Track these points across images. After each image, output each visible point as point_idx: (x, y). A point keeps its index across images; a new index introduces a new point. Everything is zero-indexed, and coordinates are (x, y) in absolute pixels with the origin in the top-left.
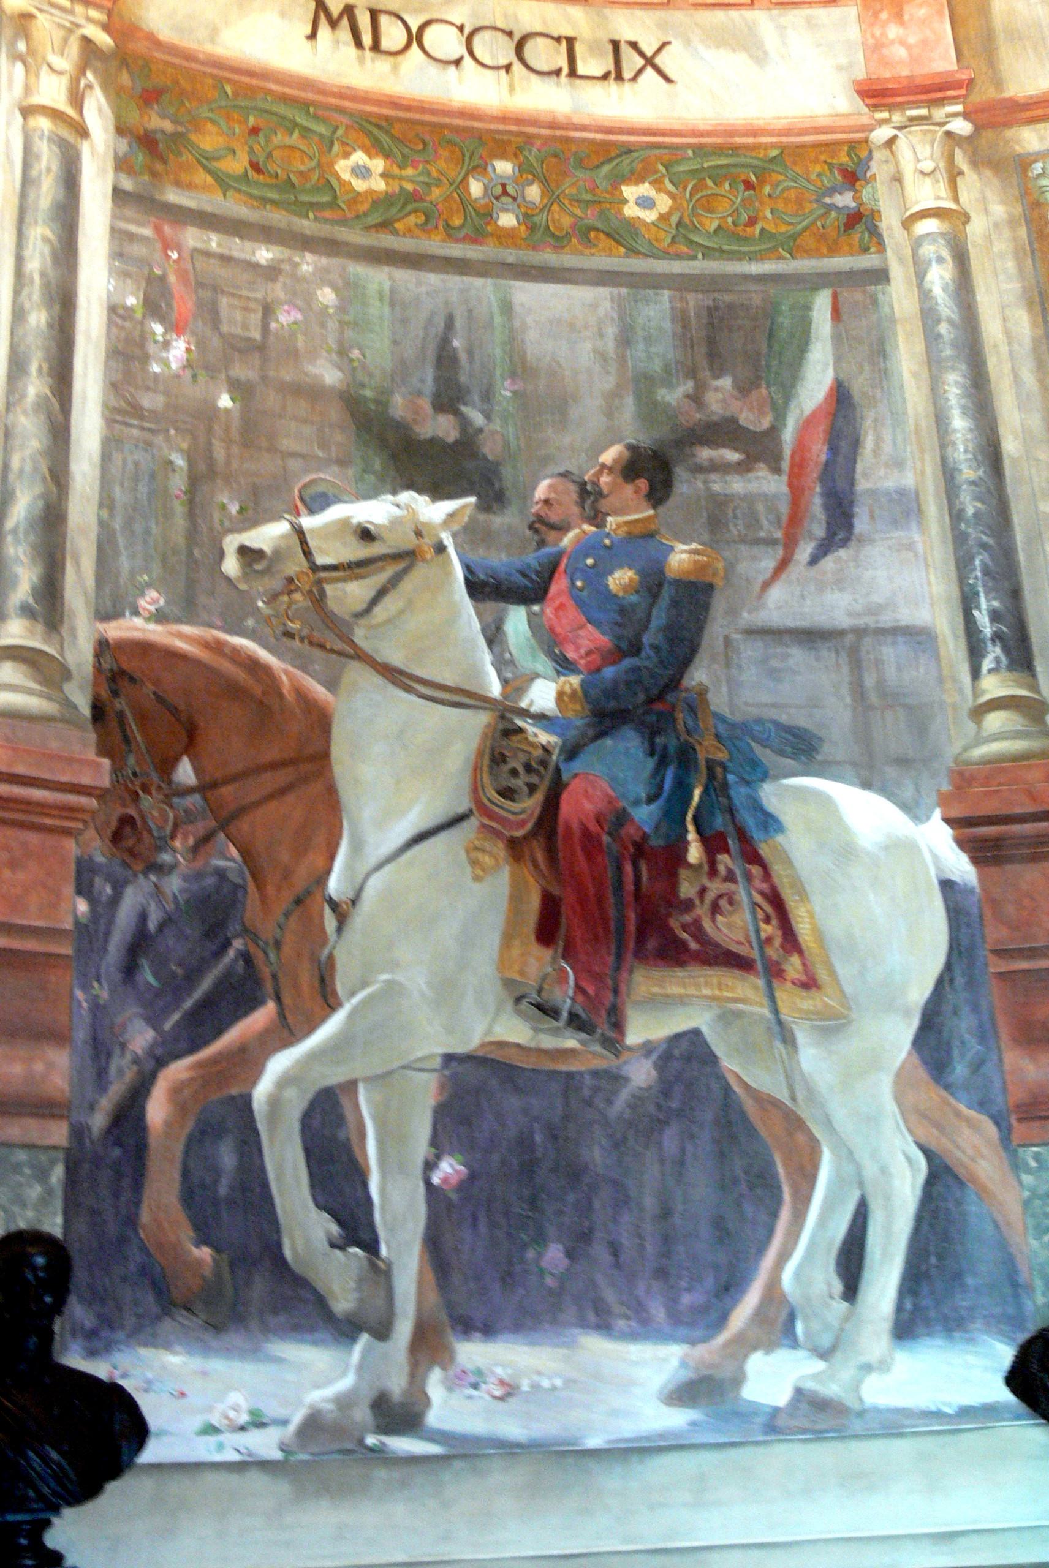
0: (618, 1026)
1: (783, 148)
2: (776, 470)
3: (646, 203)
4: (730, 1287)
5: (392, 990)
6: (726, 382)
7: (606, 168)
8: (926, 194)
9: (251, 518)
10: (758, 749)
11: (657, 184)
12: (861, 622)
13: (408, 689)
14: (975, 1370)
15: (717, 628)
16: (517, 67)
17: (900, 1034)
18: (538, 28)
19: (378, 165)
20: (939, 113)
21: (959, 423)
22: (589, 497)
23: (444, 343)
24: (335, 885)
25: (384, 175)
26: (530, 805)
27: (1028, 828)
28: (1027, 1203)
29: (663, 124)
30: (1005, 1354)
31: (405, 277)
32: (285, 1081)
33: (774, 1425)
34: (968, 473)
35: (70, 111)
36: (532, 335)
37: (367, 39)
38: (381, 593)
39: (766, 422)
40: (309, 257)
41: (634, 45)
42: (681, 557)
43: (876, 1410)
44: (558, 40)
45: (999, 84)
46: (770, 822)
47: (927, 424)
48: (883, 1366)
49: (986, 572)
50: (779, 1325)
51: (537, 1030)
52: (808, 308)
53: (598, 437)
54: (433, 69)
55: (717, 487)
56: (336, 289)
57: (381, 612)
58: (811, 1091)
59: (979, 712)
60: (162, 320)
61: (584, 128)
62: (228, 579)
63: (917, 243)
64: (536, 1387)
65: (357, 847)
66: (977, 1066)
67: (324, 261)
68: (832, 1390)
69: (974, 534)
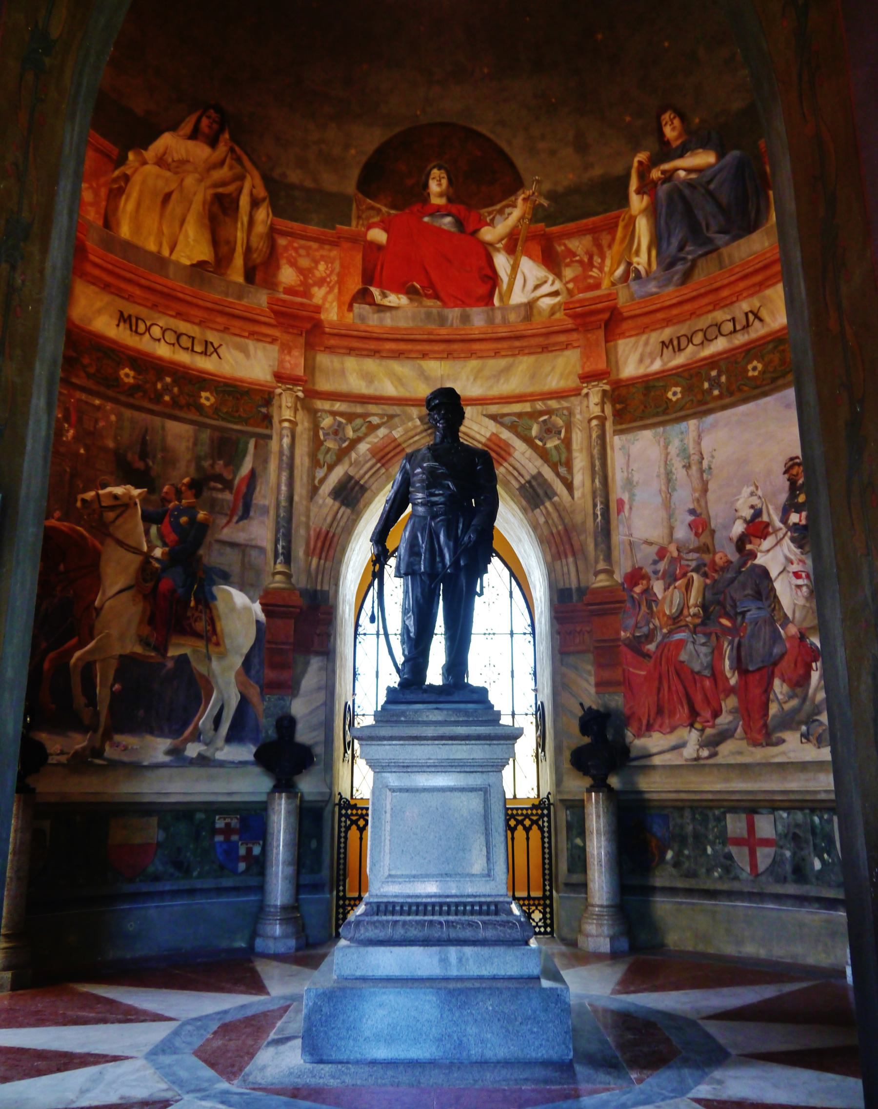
0: (166, 651)
2: (231, 493)
3: (207, 399)
5: (108, 636)
6: (221, 462)
9: (85, 491)
11: (212, 394)
13: (122, 547)
14: (246, 752)
15: (209, 539)
16: (177, 345)
18: (184, 332)
19: (132, 373)
21: (284, 488)
22: (179, 494)
23: (144, 438)
24: (97, 603)
26: (150, 585)
30: (254, 749)
31: (136, 414)
32: (79, 659)
34: (283, 503)
37: (134, 328)
40: (109, 404)
41: (212, 343)
42: (201, 515)
44: (189, 337)
45: (314, 384)
46: (214, 598)
47: (275, 486)
49: (283, 533)
52: (247, 443)
54: (152, 342)
56: (115, 415)
57: (118, 523)
59: (274, 574)
60: (67, 423)
61: (193, 370)
63: (282, 428)
67: (114, 406)
68: (208, 754)
69: (283, 523)
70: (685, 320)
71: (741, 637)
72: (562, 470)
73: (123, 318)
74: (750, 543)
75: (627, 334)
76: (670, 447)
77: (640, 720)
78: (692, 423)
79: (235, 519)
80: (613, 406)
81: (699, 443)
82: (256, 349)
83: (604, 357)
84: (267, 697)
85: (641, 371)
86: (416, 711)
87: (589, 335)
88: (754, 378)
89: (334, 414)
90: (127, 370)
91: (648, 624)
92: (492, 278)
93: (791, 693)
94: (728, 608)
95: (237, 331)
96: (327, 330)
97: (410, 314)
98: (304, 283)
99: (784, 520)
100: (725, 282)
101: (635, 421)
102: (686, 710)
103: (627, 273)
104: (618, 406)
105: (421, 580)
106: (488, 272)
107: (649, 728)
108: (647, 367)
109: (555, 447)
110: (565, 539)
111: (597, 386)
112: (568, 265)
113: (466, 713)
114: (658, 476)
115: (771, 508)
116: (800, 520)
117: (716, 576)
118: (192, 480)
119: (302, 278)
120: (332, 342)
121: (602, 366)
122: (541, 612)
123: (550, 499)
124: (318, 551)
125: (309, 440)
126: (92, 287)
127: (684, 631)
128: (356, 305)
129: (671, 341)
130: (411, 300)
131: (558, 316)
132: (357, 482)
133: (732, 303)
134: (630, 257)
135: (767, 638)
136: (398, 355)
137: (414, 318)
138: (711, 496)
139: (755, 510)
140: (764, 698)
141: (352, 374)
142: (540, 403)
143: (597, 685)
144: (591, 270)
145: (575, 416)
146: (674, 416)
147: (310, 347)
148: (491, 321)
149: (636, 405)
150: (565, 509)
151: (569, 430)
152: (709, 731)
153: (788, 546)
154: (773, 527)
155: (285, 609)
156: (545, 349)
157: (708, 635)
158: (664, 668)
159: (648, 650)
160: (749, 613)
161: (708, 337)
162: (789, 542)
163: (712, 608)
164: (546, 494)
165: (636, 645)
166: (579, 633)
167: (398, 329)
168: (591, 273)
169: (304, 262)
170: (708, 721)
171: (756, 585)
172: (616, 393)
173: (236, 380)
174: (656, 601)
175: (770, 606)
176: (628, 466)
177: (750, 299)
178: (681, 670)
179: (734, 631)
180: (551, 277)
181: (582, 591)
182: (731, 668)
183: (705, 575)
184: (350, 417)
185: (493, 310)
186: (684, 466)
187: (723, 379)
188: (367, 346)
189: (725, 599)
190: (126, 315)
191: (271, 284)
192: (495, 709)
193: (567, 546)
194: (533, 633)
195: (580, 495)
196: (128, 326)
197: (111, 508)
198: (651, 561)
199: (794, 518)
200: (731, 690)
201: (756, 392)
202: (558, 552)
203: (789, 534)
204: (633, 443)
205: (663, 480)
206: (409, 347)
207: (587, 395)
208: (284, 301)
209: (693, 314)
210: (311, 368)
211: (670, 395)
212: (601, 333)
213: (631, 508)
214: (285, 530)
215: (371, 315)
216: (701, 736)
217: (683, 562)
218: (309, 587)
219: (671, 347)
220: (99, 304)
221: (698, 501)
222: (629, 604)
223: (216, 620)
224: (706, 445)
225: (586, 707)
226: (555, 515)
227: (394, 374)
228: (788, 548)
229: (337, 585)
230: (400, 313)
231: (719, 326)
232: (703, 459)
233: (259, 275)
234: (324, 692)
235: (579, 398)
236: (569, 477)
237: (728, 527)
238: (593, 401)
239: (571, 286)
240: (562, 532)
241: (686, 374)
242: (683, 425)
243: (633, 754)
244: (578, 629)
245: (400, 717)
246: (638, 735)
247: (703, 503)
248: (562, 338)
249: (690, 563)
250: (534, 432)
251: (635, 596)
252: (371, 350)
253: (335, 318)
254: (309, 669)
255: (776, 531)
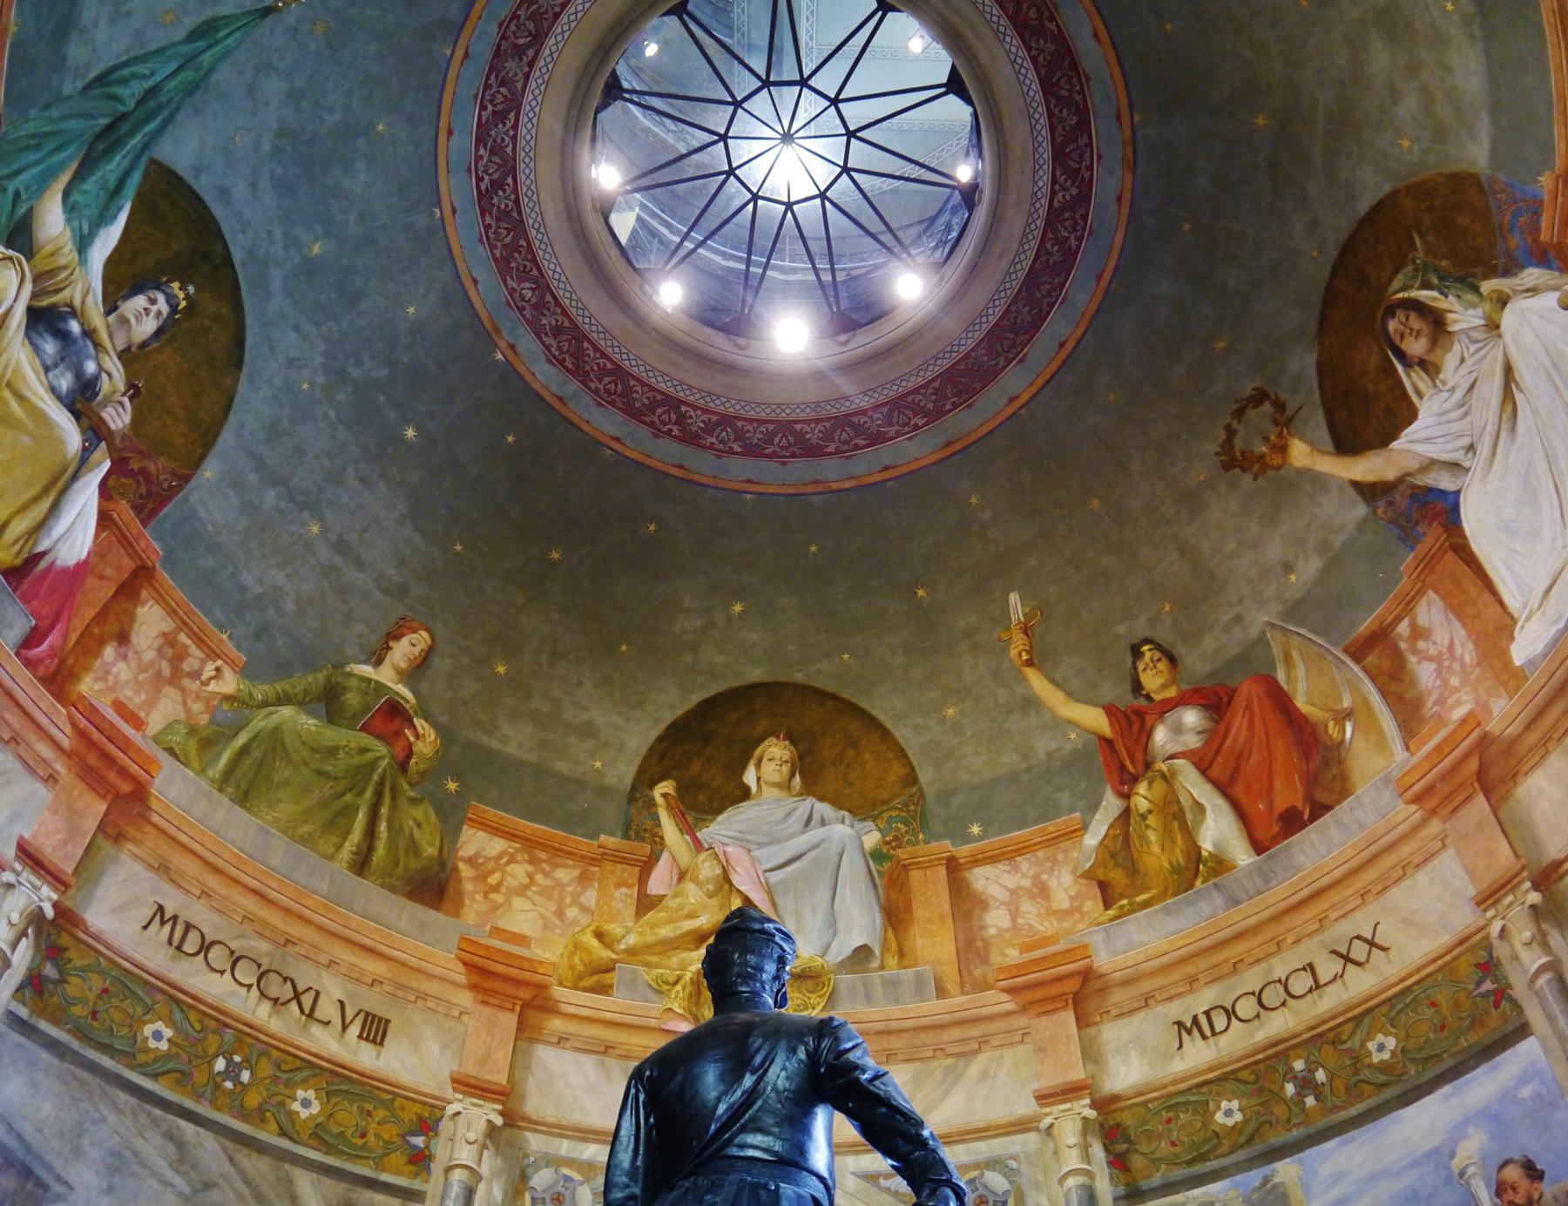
8: (465, 1155)
129: (1195, 1020)
161: (1265, 1003)
219: (1195, 1032)
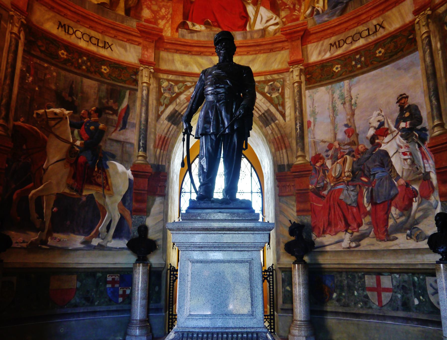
0: (82, 192)
1: (127, 66)
2: (117, 116)
3: (105, 70)
4: (92, 229)
5: (50, 183)
6: (112, 101)
7: (100, 62)
10: (107, 156)
11: (107, 67)
12: (125, 140)
13: (59, 139)
14: (122, 243)
15: (104, 138)
16: (89, 42)
17: (119, 198)
18: (94, 36)
19: (65, 53)
20: (150, 68)
21: (143, 115)
25: (66, 55)
26: (74, 159)
27: (141, 173)
28: (132, 223)
29: (110, 57)
31: (67, 73)
33: (95, 248)
34: (143, 122)
35: (18, 34)
36: (85, 87)
37: (67, 31)
38: (56, 124)
39: (117, 108)
40: (53, 67)
41: (108, 43)
42: (101, 126)
43: (109, 247)
44: (96, 39)
45: (159, 66)
46: (107, 167)
47: (139, 114)
48: (111, 241)
50: (97, 235)
51: (70, 191)
52: (126, 92)
53: (92, 105)
54: (76, 39)
55: (108, 117)
57: (57, 126)
58: (107, 204)
59: (138, 156)
61: (98, 55)
62: (34, 117)
63: (143, 86)
64: (63, 240)
65: (48, 161)
66: (129, 204)
67: (55, 68)
68: (103, 244)
69: (142, 132)
70: (343, 32)
71: (373, 186)
72: (280, 108)
73: (60, 25)
74: (378, 139)
75: (312, 41)
76: (334, 95)
77: (319, 228)
78: (346, 82)
79: (119, 129)
80: (305, 76)
81: (350, 91)
82: (130, 47)
83: (301, 52)
84: (134, 216)
85: (320, 58)
86: (207, 214)
87: (293, 43)
88: (380, 57)
89: (168, 80)
90: (63, 51)
91: (323, 181)
92: (246, 17)
93: (401, 214)
94: (366, 172)
95: (121, 38)
96: (166, 40)
97: (206, 35)
98: (155, 17)
99: (397, 126)
100: (364, 11)
101: (316, 83)
102: (343, 224)
103: (312, 12)
104: (308, 76)
105: (211, 138)
106: (244, 14)
107: (324, 232)
108: (324, 56)
109: (277, 97)
110: (281, 140)
111: (297, 67)
112: (283, 10)
113: (238, 214)
114: (328, 109)
115: (389, 121)
116: (406, 126)
117: (359, 157)
118: (97, 108)
119: (153, 15)
120: (168, 46)
121: (300, 57)
122: (268, 179)
123: (274, 122)
124: (160, 146)
125: (156, 93)
126: (44, 7)
127: (342, 185)
128: (180, 29)
129: (335, 43)
130: (206, 28)
131: (278, 34)
132: (180, 114)
133: (367, 21)
134: (314, 4)
135: (388, 186)
136: (200, 54)
137: (208, 36)
138: (356, 117)
139: (381, 123)
140: (386, 217)
141: (178, 62)
142: (269, 76)
143: (298, 211)
144: (295, 12)
145: (286, 82)
146: (337, 79)
147: (157, 48)
148: (245, 37)
149: (316, 75)
150: (281, 126)
151: (283, 89)
152: (356, 234)
153: (399, 139)
154: (391, 130)
155: (144, 174)
156: (271, 50)
157: (355, 186)
158: (332, 202)
159: (324, 194)
160: (377, 174)
161: (355, 39)
162: (400, 137)
163: (357, 172)
164: (272, 119)
165: (317, 192)
166: (288, 186)
167: (200, 41)
168: (294, 13)
169: (155, 8)
170: (355, 229)
171: (381, 160)
172: (307, 70)
173: (119, 61)
174: (328, 170)
175: (389, 170)
176: (313, 105)
177: (378, 18)
178: (340, 203)
179: (369, 184)
180: (275, 16)
181: (290, 166)
182: (367, 202)
183: (353, 156)
184: (177, 82)
185: (246, 32)
186: (342, 103)
187: (363, 59)
188: (185, 49)
189: (364, 168)
190: (62, 24)
191: (138, 17)
192: (256, 212)
193: (282, 144)
194: (262, 192)
195: (289, 120)
196: (63, 29)
197: (53, 119)
198: (325, 150)
199: (403, 125)
200: (368, 213)
201: (381, 63)
202: (278, 148)
203: (400, 133)
204: (316, 94)
205: (331, 111)
206: (205, 50)
207: (292, 71)
208: (145, 26)
209: (346, 29)
210: (157, 58)
211: (334, 69)
212: (299, 42)
213: (314, 125)
214: (144, 134)
215: (187, 35)
216: (351, 236)
217: (342, 150)
218: (155, 163)
219: (335, 46)
220: (47, 16)
221: (349, 120)
222: (313, 172)
223: (108, 177)
224: (354, 92)
225: (292, 222)
226: (276, 129)
227: (198, 63)
228: (399, 140)
229: (169, 162)
230: (201, 34)
231: (360, 33)
232: (352, 99)
233: (132, 12)
234: (162, 214)
235: (288, 73)
236: (283, 111)
237: (365, 132)
238: (296, 74)
239: (284, 20)
240: (280, 138)
241: (343, 59)
242: (342, 83)
243: (316, 245)
244: (288, 184)
245: (197, 217)
246: (318, 236)
247: (352, 121)
248: (280, 45)
249: (345, 151)
250: (266, 89)
251: (317, 167)
252: (187, 51)
253: (170, 35)
254: (155, 203)
255: (392, 132)
